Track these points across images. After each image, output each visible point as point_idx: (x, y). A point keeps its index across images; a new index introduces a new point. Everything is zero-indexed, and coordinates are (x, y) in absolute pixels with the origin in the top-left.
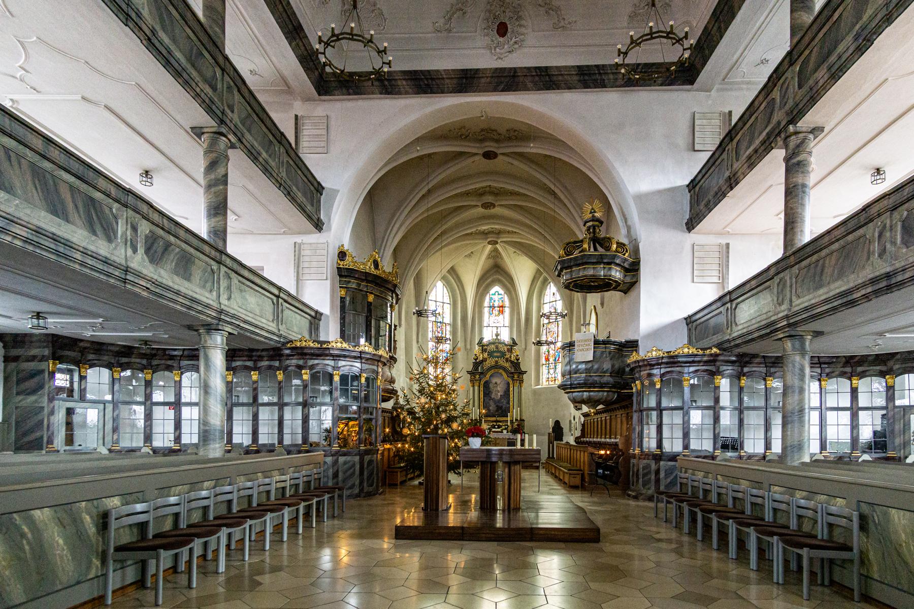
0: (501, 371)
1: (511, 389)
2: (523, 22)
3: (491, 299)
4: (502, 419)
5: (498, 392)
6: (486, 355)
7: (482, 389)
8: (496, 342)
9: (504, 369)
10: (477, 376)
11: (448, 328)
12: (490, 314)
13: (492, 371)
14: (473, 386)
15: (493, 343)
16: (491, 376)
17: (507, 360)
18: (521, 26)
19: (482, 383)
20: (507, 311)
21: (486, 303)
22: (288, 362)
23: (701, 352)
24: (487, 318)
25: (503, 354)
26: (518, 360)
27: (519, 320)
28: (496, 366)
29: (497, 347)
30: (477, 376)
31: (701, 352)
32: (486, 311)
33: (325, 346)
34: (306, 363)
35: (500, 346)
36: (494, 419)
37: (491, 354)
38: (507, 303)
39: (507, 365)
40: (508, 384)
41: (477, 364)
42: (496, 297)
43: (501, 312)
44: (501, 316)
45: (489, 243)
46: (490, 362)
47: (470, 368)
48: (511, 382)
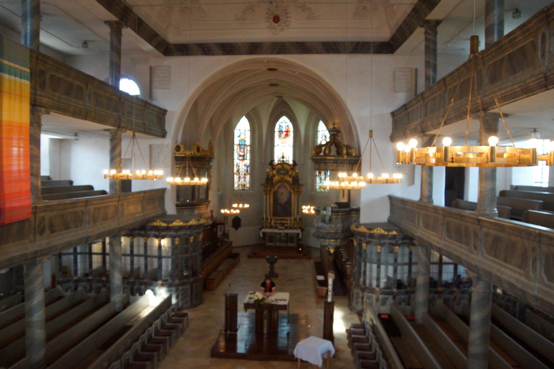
0: (286, 184)
1: (293, 197)
2: (288, 15)
3: (280, 126)
4: (285, 218)
5: (283, 198)
6: (275, 172)
7: (272, 196)
8: (283, 164)
9: (287, 182)
10: (269, 188)
11: (249, 148)
12: (280, 136)
13: (279, 184)
14: (266, 194)
15: (280, 164)
16: (279, 187)
17: (290, 176)
18: (287, 17)
19: (272, 192)
20: (291, 134)
21: (277, 129)
22: (149, 232)
23: (386, 233)
24: (277, 140)
25: (287, 173)
26: (297, 177)
27: (300, 142)
28: (282, 181)
29: (283, 167)
30: (269, 188)
31: (386, 233)
32: (277, 134)
33: (170, 225)
34: (160, 234)
35: (285, 166)
36: (280, 218)
37: (278, 171)
38: (291, 129)
39: (290, 180)
40: (290, 193)
41: (269, 180)
42: (284, 125)
43: (287, 135)
44: (287, 138)
45: (277, 97)
46: (276, 178)
47: (264, 182)
48: (292, 192)
